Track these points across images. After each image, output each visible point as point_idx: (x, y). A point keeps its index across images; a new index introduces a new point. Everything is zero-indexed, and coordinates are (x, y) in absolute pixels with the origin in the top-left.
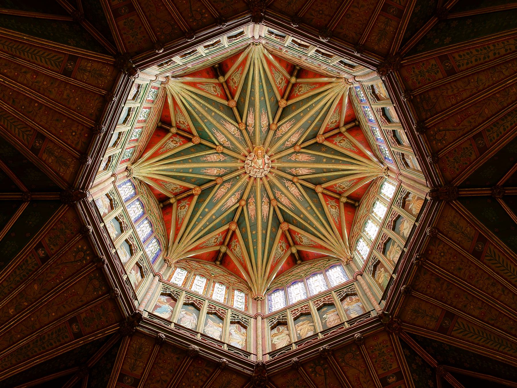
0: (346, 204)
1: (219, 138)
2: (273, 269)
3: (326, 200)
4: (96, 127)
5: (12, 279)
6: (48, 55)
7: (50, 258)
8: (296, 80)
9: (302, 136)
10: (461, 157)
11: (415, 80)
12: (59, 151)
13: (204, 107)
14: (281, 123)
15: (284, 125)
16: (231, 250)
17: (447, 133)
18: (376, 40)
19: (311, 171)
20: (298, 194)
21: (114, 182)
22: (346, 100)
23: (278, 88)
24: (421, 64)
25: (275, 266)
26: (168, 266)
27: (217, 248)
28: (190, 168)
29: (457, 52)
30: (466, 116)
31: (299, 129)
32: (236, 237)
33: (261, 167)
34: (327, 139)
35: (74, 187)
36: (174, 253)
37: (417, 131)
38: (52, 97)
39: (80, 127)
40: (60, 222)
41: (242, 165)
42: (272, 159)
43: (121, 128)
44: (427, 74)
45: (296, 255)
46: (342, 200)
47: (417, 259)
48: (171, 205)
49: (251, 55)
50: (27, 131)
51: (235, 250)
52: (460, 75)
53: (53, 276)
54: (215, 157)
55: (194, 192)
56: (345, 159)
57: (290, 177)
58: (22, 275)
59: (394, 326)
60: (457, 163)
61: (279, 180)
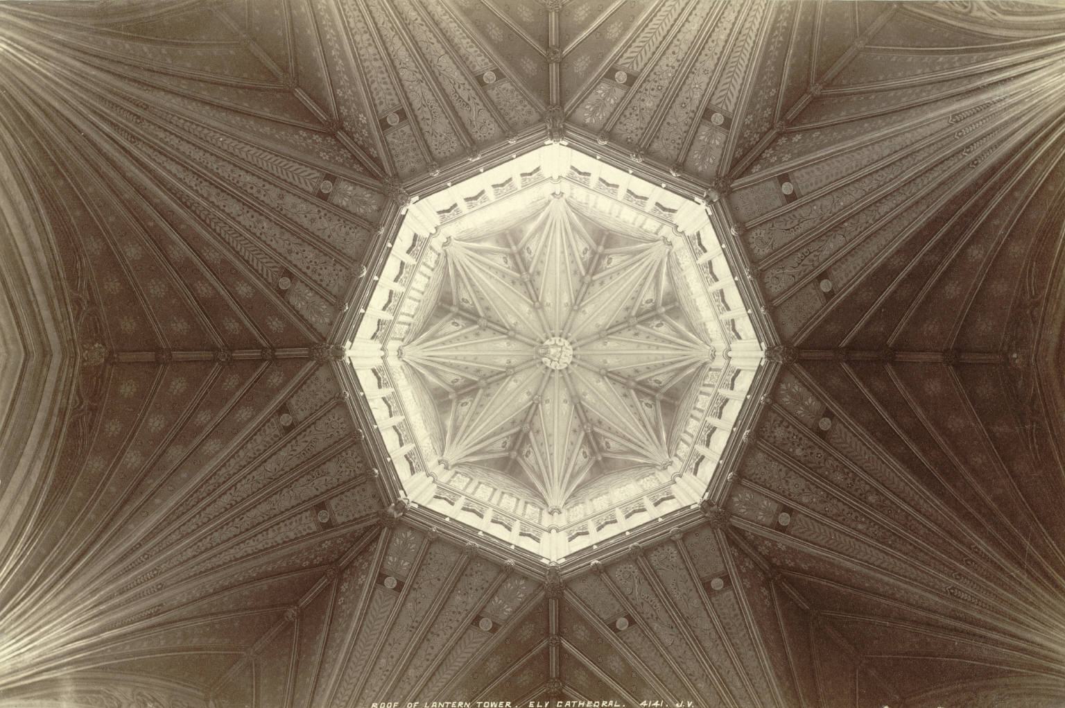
2: (683, 337)
11: (413, 160)
33: (560, 349)
41: (557, 372)
45: (669, 307)
47: (637, 157)
59: (722, 186)
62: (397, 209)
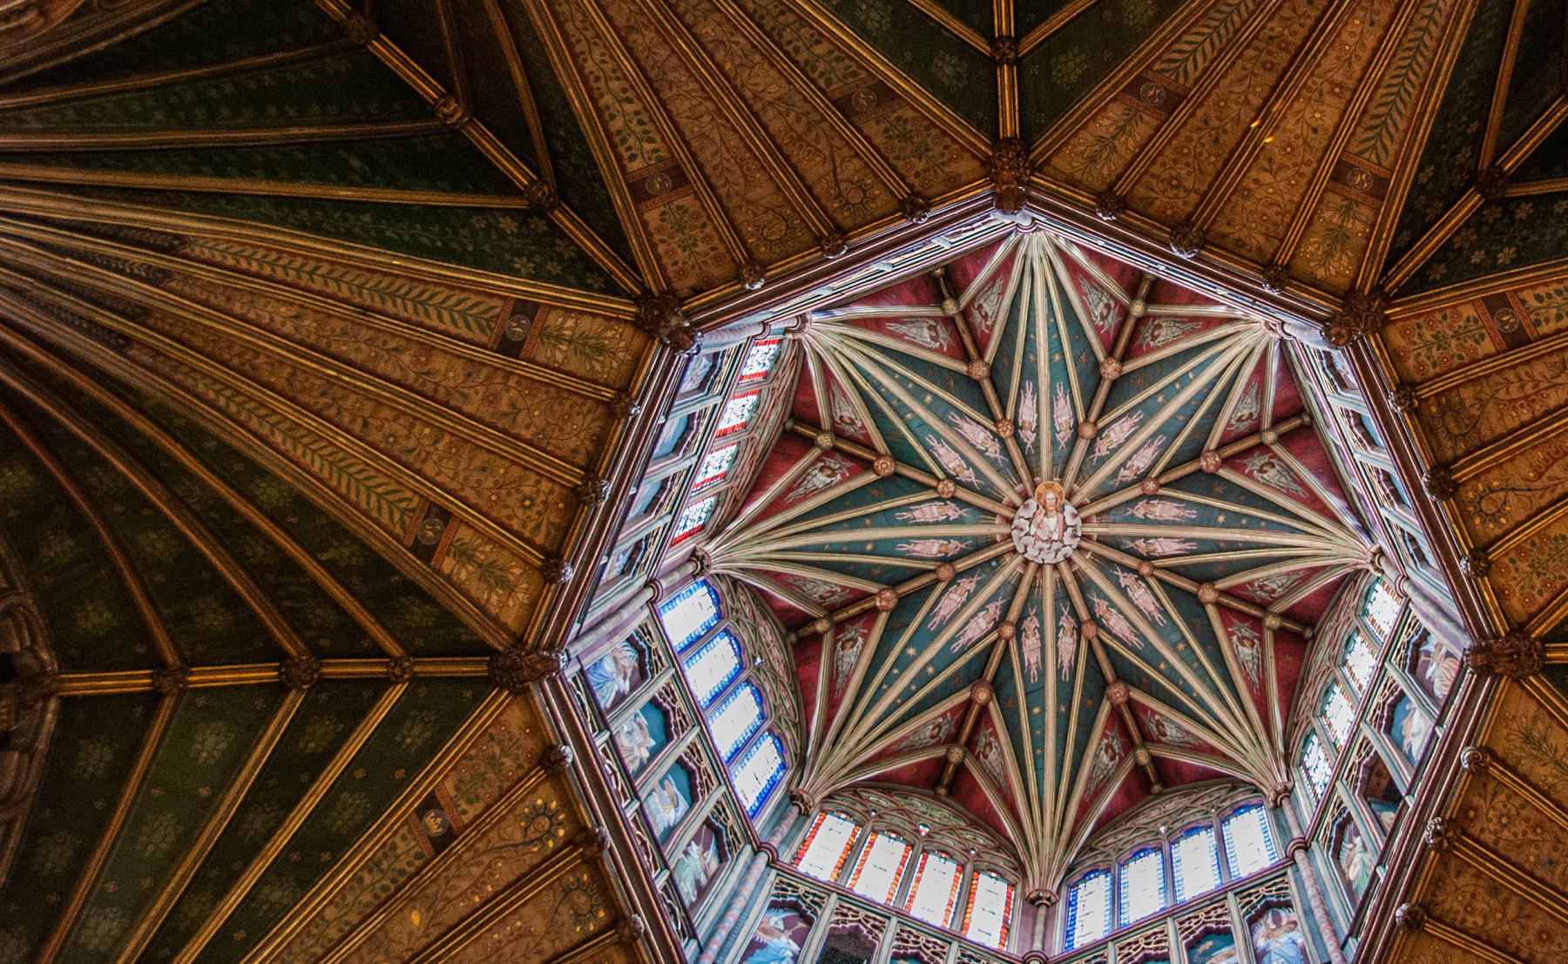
0: (1280, 634)
1: (943, 461)
2: (1085, 809)
3: (1226, 624)
4: (586, 484)
5: (350, 899)
6: (459, 303)
7: (456, 838)
8: (1146, 308)
9: (1161, 455)
10: (1548, 561)
11: (1423, 358)
12: (488, 548)
13: (902, 381)
14: (1106, 420)
15: (1116, 426)
16: (977, 757)
17: (1511, 495)
18: (1320, 253)
19: (1186, 546)
20: (1152, 608)
21: (651, 602)
22: (1274, 365)
23: (1097, 329)
24: (1438, 316)
25: (1092, 801)
26: (800, 813)
27: (940, 752)
28: (867, 542)
29: (1531, 287)
30: (1557, 453)
31: (1153, 436)
32: (990, 723)
33: (1055, 537)
34: (1227, 462)
35: (526, 643)
36: (817, 776)
37: (1432, 493)
38: (469, 408)
39: (545, 486)
40: (486, 738)
41: (1005, 530)
42: (1084, 514)
43: (660, 470)
44: (1454, 343)
45: (1150, 770)
46: (1268, 623)
48: (817, 638)
49: (1022, 249)
50: (401, 500)
51: (986, 757)
52: (1542, 347)
53: (465, 885)
54: (933, 512)
55: (878, 604)
56: (1274, 518)
57: (1131, 562)
58: (378, 886)
60: (1539, 574)
61: (1101, 569)
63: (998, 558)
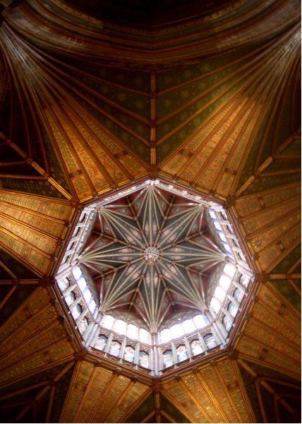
13: (183, 289)
27: (175, 205)
31: (128, 275)
57: (133, 247)
62: (88, 353)
63: (162, 247)
